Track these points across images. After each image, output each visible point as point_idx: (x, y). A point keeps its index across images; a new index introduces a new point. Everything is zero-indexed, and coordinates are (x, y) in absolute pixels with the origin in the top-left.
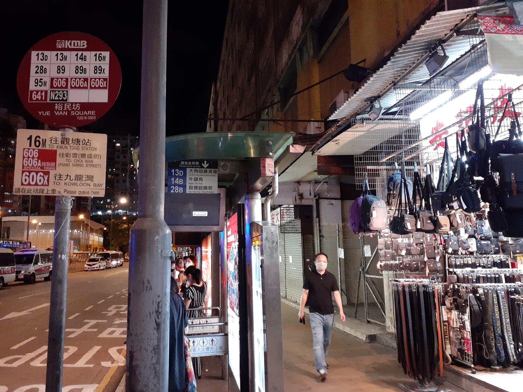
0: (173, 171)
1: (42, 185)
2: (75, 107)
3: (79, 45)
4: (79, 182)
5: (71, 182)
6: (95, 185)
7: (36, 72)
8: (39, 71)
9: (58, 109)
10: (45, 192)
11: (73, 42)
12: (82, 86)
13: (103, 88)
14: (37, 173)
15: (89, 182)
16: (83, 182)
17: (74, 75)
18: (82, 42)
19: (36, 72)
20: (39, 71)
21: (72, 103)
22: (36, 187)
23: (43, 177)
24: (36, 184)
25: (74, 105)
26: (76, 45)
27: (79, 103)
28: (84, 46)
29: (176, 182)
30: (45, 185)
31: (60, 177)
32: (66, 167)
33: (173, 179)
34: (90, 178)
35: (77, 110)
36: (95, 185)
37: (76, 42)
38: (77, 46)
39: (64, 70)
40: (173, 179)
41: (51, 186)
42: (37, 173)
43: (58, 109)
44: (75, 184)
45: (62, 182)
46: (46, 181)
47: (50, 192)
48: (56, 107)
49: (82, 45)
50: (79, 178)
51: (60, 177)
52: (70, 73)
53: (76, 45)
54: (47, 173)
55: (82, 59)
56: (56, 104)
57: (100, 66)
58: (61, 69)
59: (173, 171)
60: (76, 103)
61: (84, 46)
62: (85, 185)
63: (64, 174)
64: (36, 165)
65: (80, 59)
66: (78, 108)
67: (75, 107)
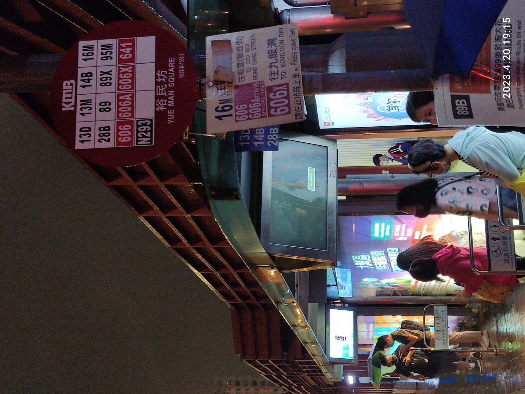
0: (241, 144)
1: (288, 90)
2: (162, 77)
3: (70, 91)
4: (279, 53)
5: (279, 61)
6: (280, 36)
7: (109, 140)
8: (106, 138)
9: (165, 106)
10: (297, 85)
11: (64, 100)
12: (131, 75)
13: (133, 47)
14: (270, 100)
15: (277, 43)
16: (278, 48)
17: (113, 88)
18: (64, 87)
19: (109, 140)
20: (106, 138)
21: (157, 83)
22: (292, 104)
23: (275, 92)
24: (287, 97)
25: (160, 80)
26: (70, 95)
27: (156, 72)
28: (71, 84)
29: (261, 139)
30: (288, 87)
31: (274, 73)
32: (259, 71)
33: (256, 144)
34: (271, 42)
35: (167, 75)
36: (280, 36)
37: (65, 96)
38: (71, 93)
39: (105, 103)
40: (256, 144)
41: (289, 79)
42: (270, 100)
43: (165, 106)
44: (282, 56)
45: (281, 70)
46: (281, 88)
47: (297, 80)
48: (162, 109)
49: (71, 87)
50: (272, 54)
51: (274, 73)
52: (109, 95)
53: (70, 95)
54: (270, 89)
55: (89, 80)
56: (157, 109)
57: (101, 79)
58: (105, 107)
59: (241, 144)
60: (156, 77)
61: (71, 84)
62: (282, 45)
63: (268, 70)
64: (259, 104)
65: (89, 82)
66: (164, 73)
67: (162, 77)
